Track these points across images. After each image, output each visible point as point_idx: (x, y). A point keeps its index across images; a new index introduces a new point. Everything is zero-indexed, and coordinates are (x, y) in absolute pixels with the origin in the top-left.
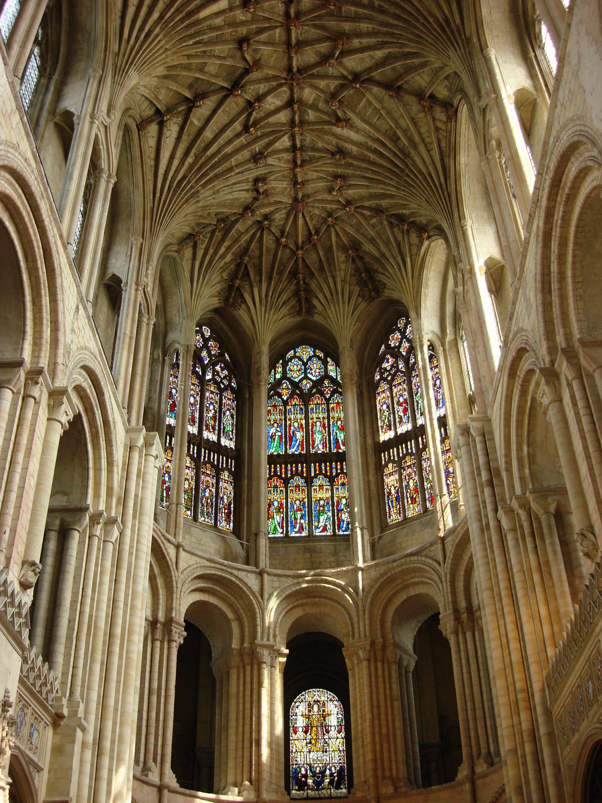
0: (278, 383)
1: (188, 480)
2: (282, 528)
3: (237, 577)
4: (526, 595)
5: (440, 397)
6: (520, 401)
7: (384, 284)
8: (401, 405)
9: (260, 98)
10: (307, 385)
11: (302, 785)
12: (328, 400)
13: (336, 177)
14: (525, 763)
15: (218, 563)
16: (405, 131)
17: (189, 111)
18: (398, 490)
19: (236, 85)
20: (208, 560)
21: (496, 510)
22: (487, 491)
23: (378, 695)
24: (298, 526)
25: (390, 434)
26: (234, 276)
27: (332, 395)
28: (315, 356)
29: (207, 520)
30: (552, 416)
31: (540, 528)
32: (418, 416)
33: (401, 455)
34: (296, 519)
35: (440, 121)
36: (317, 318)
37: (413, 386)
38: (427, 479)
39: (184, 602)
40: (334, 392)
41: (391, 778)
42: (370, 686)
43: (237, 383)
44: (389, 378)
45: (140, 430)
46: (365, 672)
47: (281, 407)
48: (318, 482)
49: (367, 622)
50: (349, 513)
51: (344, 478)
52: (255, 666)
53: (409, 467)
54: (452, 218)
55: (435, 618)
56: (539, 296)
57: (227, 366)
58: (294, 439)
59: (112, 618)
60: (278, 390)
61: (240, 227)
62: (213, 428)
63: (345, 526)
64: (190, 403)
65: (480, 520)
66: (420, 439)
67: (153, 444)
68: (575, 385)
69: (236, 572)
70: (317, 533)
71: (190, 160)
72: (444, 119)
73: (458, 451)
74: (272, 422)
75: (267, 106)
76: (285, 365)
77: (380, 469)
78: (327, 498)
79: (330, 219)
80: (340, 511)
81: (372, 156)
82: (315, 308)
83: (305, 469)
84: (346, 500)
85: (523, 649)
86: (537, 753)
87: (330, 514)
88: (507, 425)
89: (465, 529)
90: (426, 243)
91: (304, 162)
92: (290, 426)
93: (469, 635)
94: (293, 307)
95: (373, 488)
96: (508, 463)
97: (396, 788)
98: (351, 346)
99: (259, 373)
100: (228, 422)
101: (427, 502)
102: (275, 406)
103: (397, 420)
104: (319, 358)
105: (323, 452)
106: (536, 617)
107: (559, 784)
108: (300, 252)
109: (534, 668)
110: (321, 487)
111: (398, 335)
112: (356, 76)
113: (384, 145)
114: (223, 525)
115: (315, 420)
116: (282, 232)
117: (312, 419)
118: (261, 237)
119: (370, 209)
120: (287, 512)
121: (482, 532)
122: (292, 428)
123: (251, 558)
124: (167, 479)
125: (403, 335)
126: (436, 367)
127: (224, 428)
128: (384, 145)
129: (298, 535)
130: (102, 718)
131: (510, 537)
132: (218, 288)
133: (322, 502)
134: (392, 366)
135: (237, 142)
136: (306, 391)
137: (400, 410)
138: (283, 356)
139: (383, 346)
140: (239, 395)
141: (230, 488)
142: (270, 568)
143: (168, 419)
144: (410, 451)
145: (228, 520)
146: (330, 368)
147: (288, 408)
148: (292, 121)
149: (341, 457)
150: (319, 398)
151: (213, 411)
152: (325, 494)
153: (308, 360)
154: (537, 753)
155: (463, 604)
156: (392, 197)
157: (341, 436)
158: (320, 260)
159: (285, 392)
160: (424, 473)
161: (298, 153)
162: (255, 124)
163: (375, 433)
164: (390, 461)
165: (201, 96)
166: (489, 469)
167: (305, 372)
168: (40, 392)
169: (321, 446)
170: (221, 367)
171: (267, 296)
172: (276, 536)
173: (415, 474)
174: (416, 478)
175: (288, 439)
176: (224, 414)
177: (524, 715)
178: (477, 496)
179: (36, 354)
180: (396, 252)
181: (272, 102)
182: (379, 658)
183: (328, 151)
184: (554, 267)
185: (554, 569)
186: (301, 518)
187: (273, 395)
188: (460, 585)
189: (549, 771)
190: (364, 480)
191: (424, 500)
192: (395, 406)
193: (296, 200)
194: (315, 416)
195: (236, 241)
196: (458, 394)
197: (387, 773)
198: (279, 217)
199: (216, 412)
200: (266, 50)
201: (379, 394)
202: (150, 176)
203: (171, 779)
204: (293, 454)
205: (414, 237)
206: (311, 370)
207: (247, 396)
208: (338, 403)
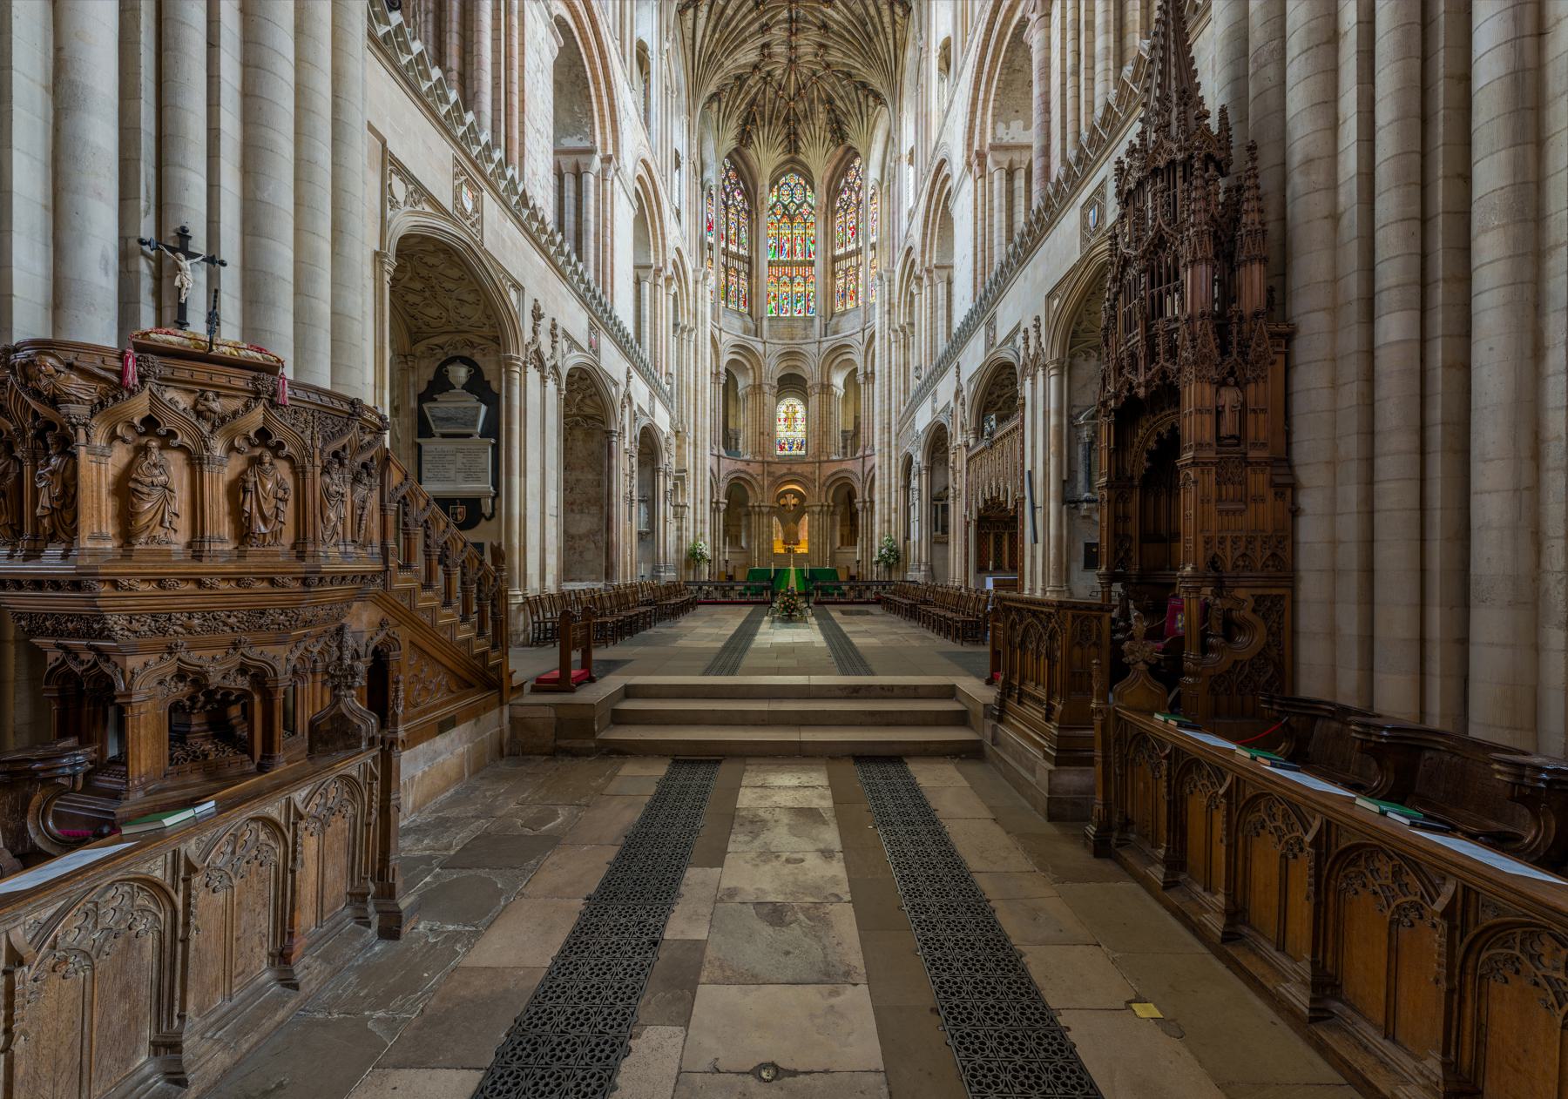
0: (775, 205)
13: (821, 46)
16: (872, 18)
26: (746, 122)
36: (801, 157)
39: (725, 358)
48: (797, 281)
55: (855, 370)
59: (696, 381)
61: (750, 82)
70: (796, 314)
77: (834, 274)
81: (847, 36)
85: (890, 404)
86: (890, 452)
100: (743, 235)
107: (897, 467)
109: (893, 414)
114: (742, 309)
116: (780, 85)
130: (695, 431)
132: (736, 132)
135: (750, 17)
138: (777, 183)
140: (749, 213)
154: (890, 452)
155: (869, 369)
157: (812, 248)
168: (661, 281)
175: (780, 249)
179: (657, 259)
183: (815, 25)
188: (870, 358)
189: (893, 461)
195: (747, 93)
198: (778, 72)
202: (689, 56)
203: (723, 452)
205: (871, 99)
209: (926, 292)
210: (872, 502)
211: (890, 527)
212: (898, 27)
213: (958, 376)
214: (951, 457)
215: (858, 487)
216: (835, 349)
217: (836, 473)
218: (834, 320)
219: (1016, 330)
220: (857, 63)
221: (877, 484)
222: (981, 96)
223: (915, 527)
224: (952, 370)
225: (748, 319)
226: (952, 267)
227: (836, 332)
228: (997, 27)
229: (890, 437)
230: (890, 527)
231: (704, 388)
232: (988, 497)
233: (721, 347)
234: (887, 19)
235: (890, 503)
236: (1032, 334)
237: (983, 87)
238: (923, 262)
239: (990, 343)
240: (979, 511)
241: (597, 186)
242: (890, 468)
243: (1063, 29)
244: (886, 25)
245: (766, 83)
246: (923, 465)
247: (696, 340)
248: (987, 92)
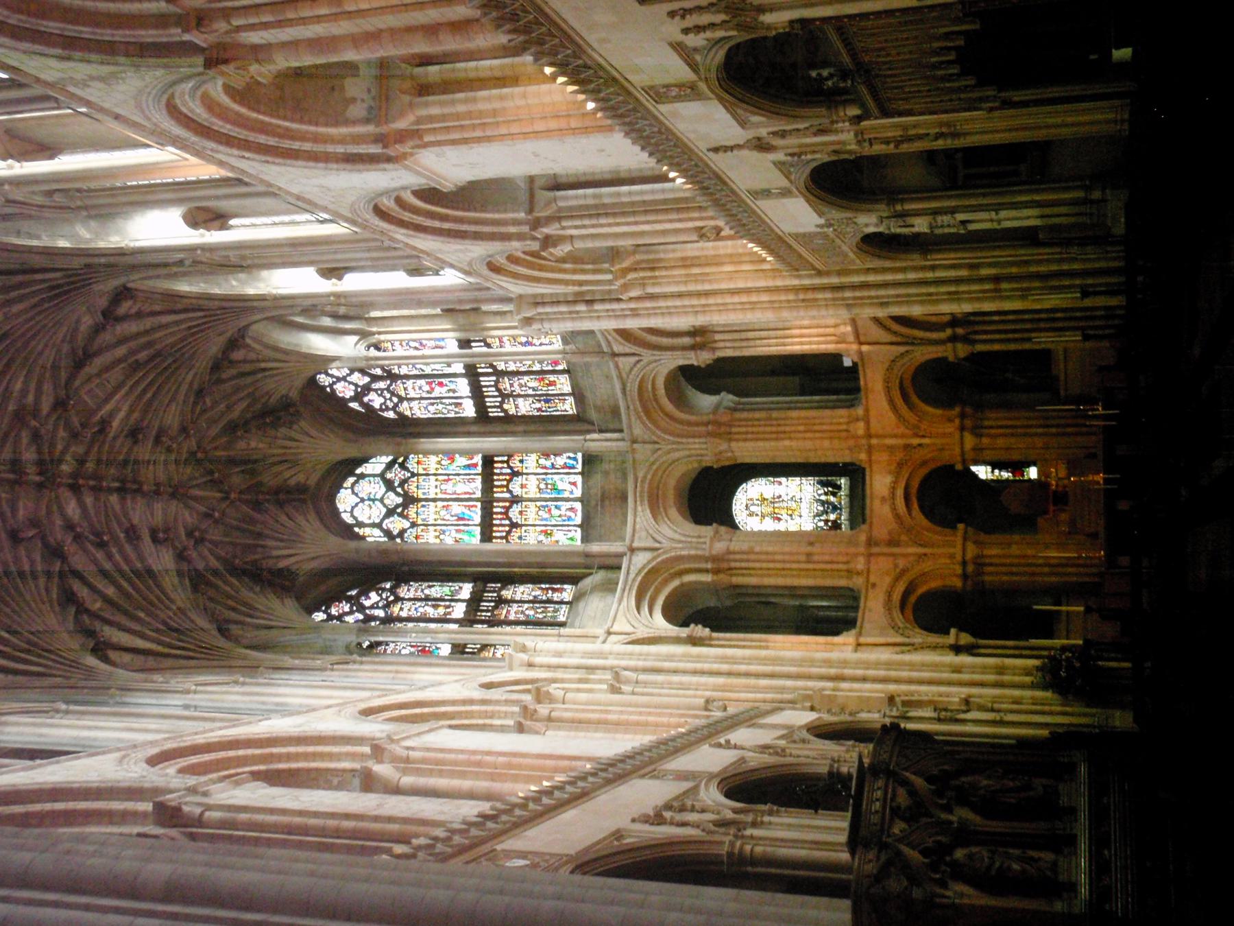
3: (637, 575)
4: (710, 281)
6: (523, 266)
7: (282, 397)
8: (433, 389)
9: (70, 526)
10: (393, 499)
11: (836, 526)
12: (413, 475)
13: (157, 440)
14: (861, 298)
16: (133, 352)
17: (87, 611)
19: (56, 552)
21: (619, 300)
22: (597, 307)
23: (764, 433)
24: (569, 513)
27: (407, 469)
30: (579, 245)
31: (648, 261)
35: (130, 308)
36: (312, 482)
40: (403, 466)
41: (848, 423)
42: (757, 440)
43: (386, 580)
46: (741, 444)
48: (517, 491)
49: (691, 440)
52: (732, 557)
53: (511, 385)
54: (255, 308)
56: (467, 242)
57: (365, 593)
65: (626, 316)
68: (565, 223)
69: (632, 576)
70: (578, 493)
71: (142, 615)
72: (130, 303)
75: (76, 517)
77: (508, 419)
79: (199, 455)
80: (553, 466)
81: (149, 395)
82: (298, 484)
85: (758, 290)
86: (853, 287)
87: (556, 477)
88: (538, 280)
90: (248, 341)
91: (134, 481)
93: (718, 337)
94: (294, 507)
95: (532, 427)
96: (574, 283)
97: (858, 420)
98: (356, 441)
100: (437, 590)
103: (451, 394)
104: (356, 482)
106: (731, 276)
107: (884, 270)
108: (233, 496)
109: (779, 283)
111: (339, 387)
112: (60, 405)
113: (137, 382)
115: (438, 490)
116: (208, 516)
118: (211, 542)
119: (195, 403)
121: (638, 315)
122: (448, 517)
123: (612, 565)
128: (137, 382)
129: (579, 514)
131: (650, 290)
133: (542, 486)
136: (400, 500)
137: (438, 391)
138: (349, 528)
141: (521, 588)
145: (561, 590)
146: (368, 472)
147: (420, 522)
148: (93, 488)
149: (488, 462)
152: (532, 482)
154: (853, 287)
155: (687, 341)
156: (196, 374)
158: (243, 471)
160: (522, 369)
161: (129, 485)
162: (98, 534)
163: (462, 421)
165: (69, 598)
166: (575, 302)
167: (373, 500)
168: (543, 710)
169: (473, 485)
171: (282, 540)
174: (526, 378)
177: (820, 296)
178: (599, 317)
180: (249, 380)
181: (72, 509)
182: (728, 429)
183: (131, 449)
184: (446, 226)
185: (690, 254)
188: (665, 341)
189: (871, 278)
193: (173, 495)
197: (844, 427)
200: (21, 513)
204: (483, 517)
205: (238, 355)
209: (571, 228)
210: (955, 321)
211: (1010, 278)
212: (147, 308)
213: (732, 148)
214: (878, 149)
215: (923, 354)
216: (647, 412)
217: (891, 402)
218: (593, 415)
219: (678, 47)
220: (186, 379)
221: (916, 311)
222: (307, 146)
223: (1011, 219)
224: (720, 162)
225: (587, 583)
226: (531, 179)
227: (615, 412)
228: (227, 128)
229: (823, 288)
230: (1010, 278)
231: (724, 659)
232: (954, 70)
233: (642, 632)
234: (132, 327)
235: (958, 281)
236: (691, 21)
237: (296, 145)
238: (520, 237)
239: (688, 92)
240: (981, 84)
241: (418, 772)
242: (885, 285)
243: (280, 24)
244: (142, 328)
245: (200, 541)
246: (883, 209)
247: (635, 670)
248: (303, 137)
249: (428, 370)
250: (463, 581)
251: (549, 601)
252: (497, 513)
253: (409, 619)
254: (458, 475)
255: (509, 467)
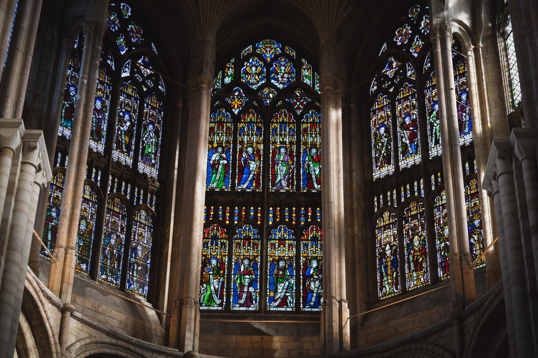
0: (228, 90)
1: (85, 218)
2: (221, 298)
5: (466, 118)
8: (407, 128)
15: (122, 339)
18: (396, 250)
20: (109, 334)
24: (245, 296)
25: (388, 170)
27: (305, 111)
28: (284, 54)
29: (109, 278)
32: (432, 144)
33: (403, 200)
34: (242, 285)
37: (427, 102)
38: (441, 236)
44: (391, 90)
45: (17, 125)
47: (229, 125)
50: (321, 281)
51: (317, 231)
53: (414, 217)
58: (246, 170)
60: (227, 99)
62: (128, 147)
63: (313, 299)
64: (95, 109)
66: (433, 177)
67: (35, 148)
70: (273, 307)
73: (494, 182)
74: (215, 145)
76: (238, 66)
78: (290, 258)
80: (308, 277)
83: (259, 215)
84: (318, 262)
87: (293, 281)
89: (495, 303)
92: (241, 152)
99: (200, 72)
101: (439, 269)
102: (220, 123)
103: (400, 149)
104: (290, 58)
105: (287, 190)
110: (282, 241)
115: (278, 146)
117: (275, 143)
120: (229, 275)
122: (244, 155)
124: (54, 214)
125: (416, 30)
126: (462, 75)
127: (144, 149)
129: (244, 309)
133: (282, 264)
134: (397, 73)
137: (405, 136)
138: (237, 54)
139: (385, 45)
141: (147, 235)
142: (199, 352)
143: (60, 129)
144: (416, 194)
147: (240, 125)
150: (286, 115)
151: (128, 124)
153: (273, 60)
159: (236, 103)
164: (386, 208)
167: (268, 78)
169: (284, 183)
170: (143, 61)
172: (211, 308)
173: (423, 229)
176: (145, 129)
186: (250, 285)
187: (219, 107)
190: (346, 232)
191: (434, 266)
192: (398, 129)
194: (279, 139)
196: (493, 115)
199: (132, 125)
201: (374, 111)
206: (277, 74)
207: (180, 105)
208: (313, 124)
249: (431, 119)
250: (160, 170)
251: (127, 266)
252: (248, 211)
253: (114, 102)
254: (298, 167)
255: (307, 225)
